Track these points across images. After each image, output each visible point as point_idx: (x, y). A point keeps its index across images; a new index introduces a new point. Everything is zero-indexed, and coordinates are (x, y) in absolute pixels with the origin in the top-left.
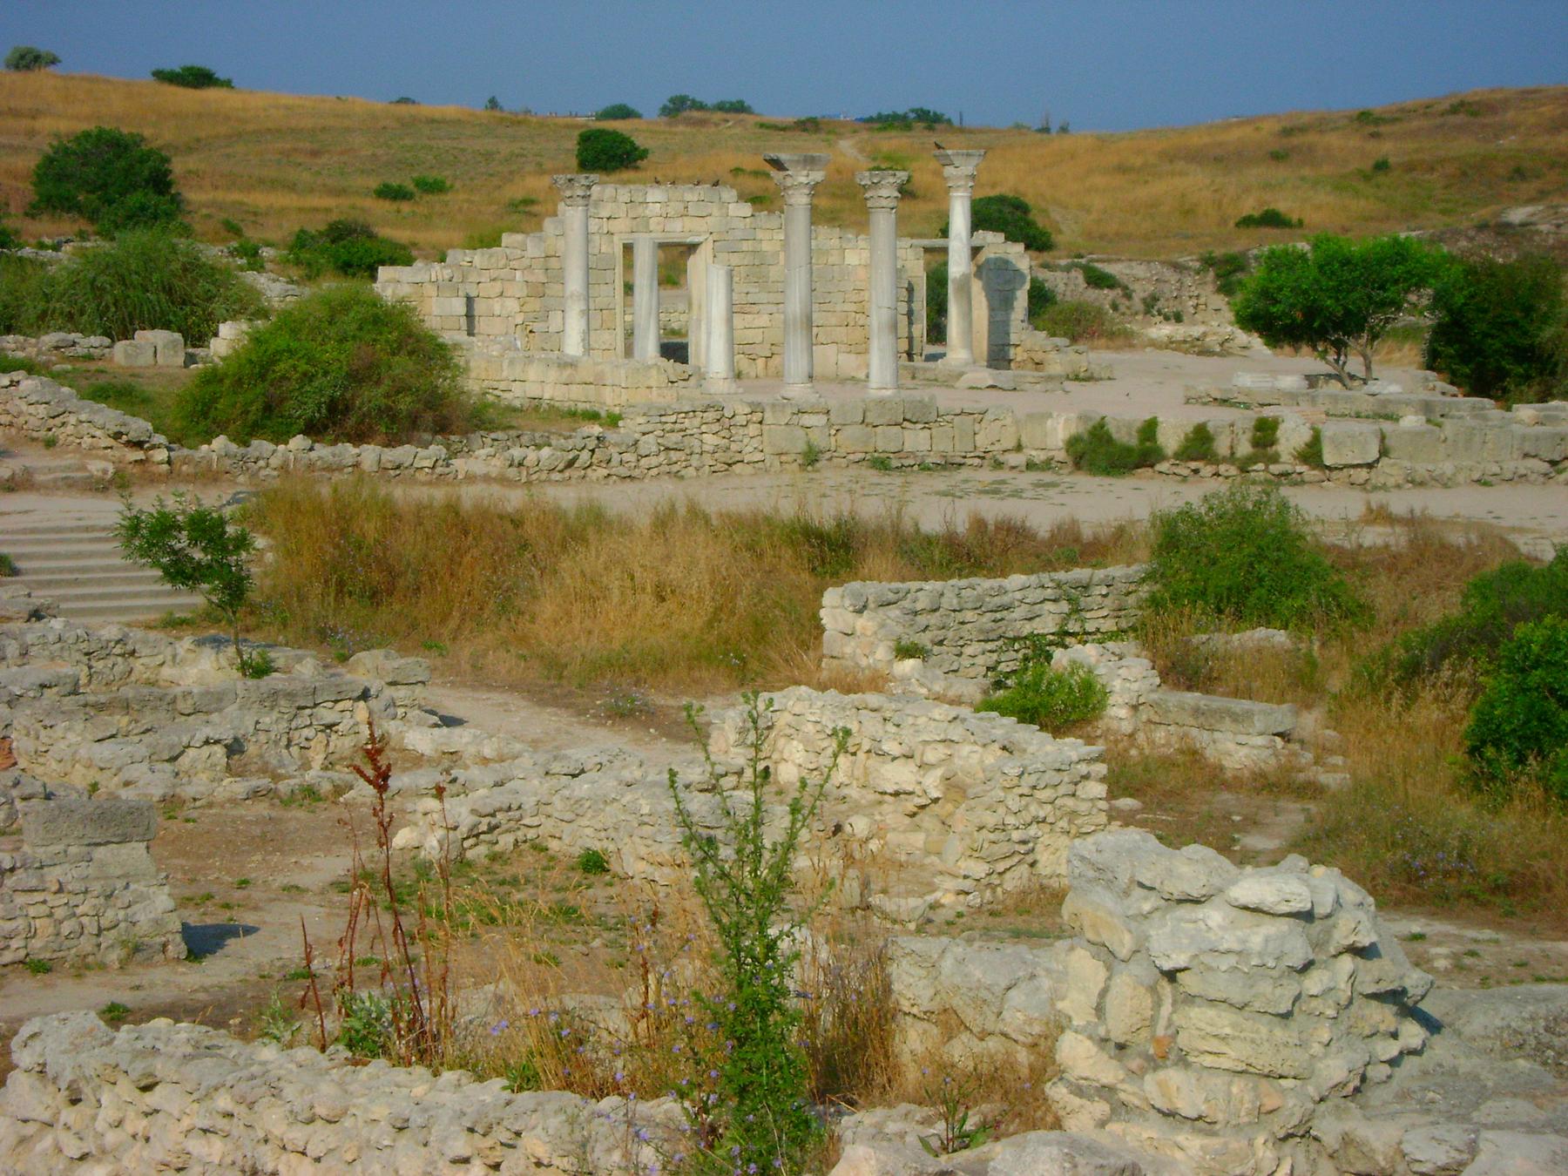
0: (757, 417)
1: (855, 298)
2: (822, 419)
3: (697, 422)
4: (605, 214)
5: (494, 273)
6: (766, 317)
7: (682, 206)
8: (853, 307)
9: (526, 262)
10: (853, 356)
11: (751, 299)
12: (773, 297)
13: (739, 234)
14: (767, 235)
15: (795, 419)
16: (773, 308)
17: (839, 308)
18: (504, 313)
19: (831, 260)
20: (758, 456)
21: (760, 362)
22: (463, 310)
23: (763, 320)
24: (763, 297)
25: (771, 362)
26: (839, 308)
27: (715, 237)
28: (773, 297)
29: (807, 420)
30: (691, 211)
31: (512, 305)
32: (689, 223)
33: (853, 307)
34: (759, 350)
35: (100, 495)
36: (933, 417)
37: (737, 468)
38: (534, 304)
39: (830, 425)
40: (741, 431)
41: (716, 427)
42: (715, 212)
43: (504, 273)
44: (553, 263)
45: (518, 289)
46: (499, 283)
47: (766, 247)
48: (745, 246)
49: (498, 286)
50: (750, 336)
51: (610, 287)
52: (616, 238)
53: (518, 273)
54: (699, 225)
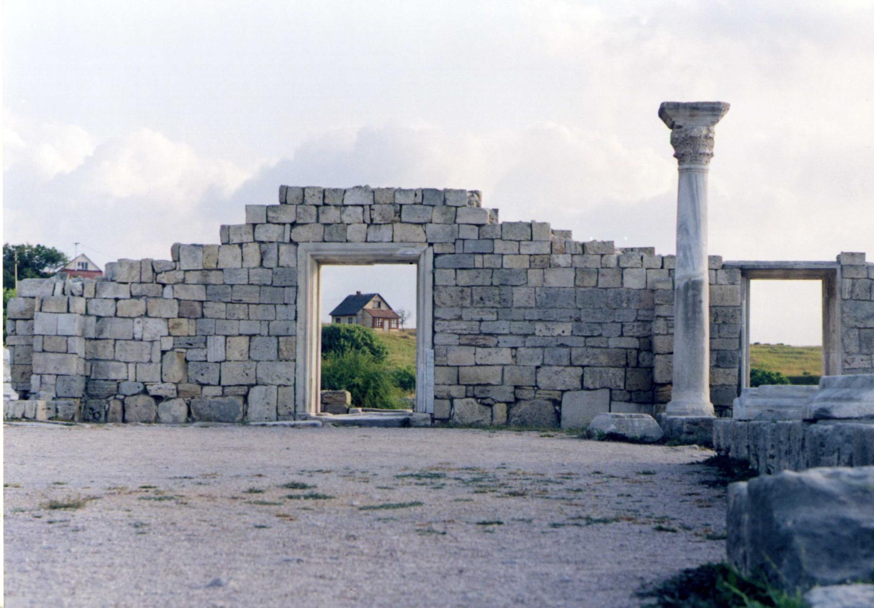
1: (638, 331)
4: (291, 219)
5: (137, 289)
8: (634, 343)
9: (180, 276)
11: (485, 328)
12: (516, 327)
13: (470, 247)
17: (613, 343)
18: (147, 336)
21: (500, 410)
24: (503, 326)
25: (515, 411)
27: (437, 249)
28: (516, 327)
30: (404, 218)
38: (187, 327)
46: (142, 301)
47: (508, 262)
49: (140, 306)
51: (291, 309)
52: (301, 247)
53: (168, 291)
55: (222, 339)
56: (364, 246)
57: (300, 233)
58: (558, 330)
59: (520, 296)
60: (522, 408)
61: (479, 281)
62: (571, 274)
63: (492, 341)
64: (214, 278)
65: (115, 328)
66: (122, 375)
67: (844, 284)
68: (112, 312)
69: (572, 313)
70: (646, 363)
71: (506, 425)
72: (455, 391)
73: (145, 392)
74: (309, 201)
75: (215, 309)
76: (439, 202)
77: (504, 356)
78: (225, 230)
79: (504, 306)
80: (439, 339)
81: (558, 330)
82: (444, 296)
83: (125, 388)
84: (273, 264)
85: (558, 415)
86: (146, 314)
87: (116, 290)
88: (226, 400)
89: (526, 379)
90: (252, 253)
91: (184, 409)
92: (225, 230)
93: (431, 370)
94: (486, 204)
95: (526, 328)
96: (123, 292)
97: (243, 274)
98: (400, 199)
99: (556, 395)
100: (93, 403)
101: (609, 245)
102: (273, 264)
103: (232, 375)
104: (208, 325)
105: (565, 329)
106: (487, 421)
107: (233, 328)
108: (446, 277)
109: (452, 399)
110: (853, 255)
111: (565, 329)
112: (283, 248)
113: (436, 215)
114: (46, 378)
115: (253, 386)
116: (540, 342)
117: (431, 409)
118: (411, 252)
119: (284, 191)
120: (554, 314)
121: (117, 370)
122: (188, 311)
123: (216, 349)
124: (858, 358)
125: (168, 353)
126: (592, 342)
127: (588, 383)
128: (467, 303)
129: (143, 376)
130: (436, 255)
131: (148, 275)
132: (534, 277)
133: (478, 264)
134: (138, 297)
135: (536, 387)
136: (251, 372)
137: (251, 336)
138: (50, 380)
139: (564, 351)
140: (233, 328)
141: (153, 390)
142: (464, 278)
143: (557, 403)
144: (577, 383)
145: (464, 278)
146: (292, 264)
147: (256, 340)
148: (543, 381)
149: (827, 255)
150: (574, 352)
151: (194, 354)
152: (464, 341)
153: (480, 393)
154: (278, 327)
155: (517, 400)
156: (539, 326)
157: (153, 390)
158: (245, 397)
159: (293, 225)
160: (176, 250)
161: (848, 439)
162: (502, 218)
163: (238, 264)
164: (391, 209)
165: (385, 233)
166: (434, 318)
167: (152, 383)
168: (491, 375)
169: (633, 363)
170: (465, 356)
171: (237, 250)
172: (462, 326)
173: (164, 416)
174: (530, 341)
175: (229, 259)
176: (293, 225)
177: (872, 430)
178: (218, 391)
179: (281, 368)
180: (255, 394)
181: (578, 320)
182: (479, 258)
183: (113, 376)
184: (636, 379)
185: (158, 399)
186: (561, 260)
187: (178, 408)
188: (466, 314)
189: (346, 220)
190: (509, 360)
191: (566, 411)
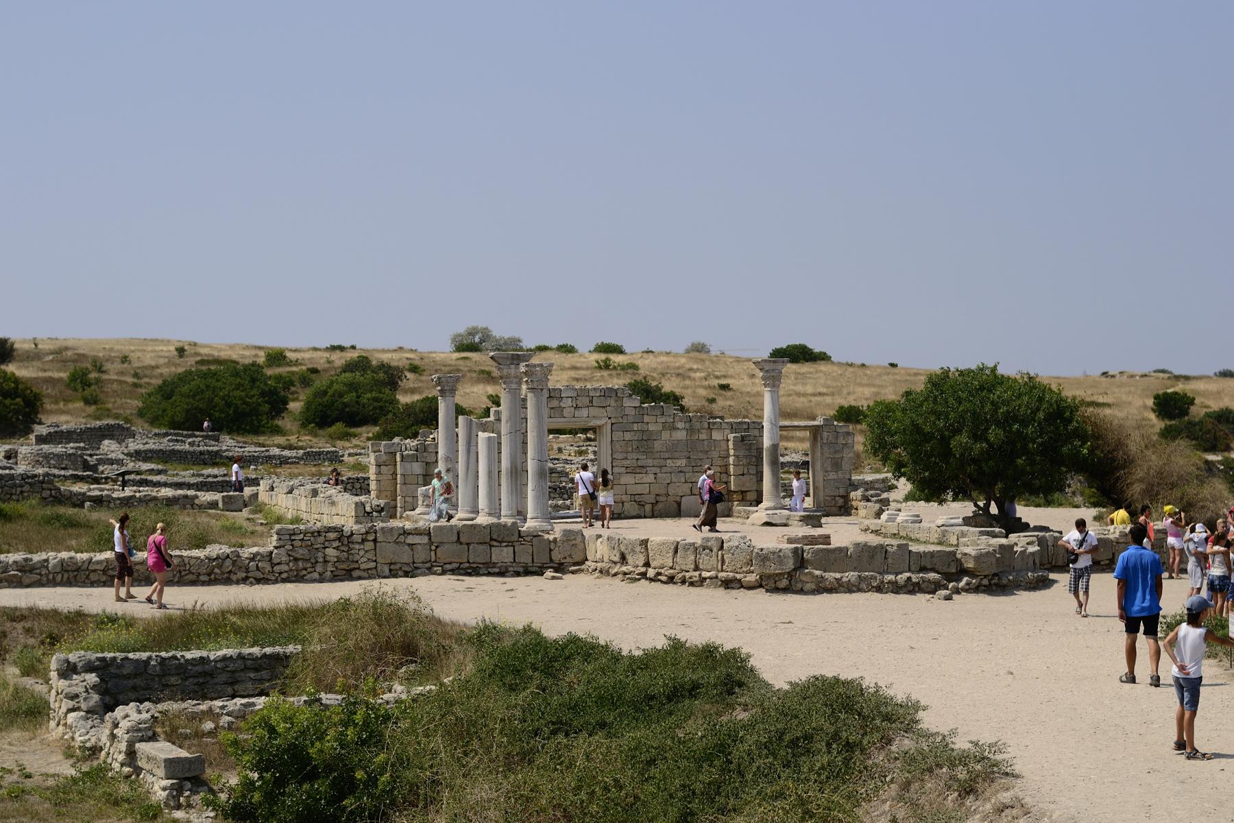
0: (371, 537)
1: (719, 462)
2: (425, 540)
3: (321, 539)
6: (652, 476)
7: (587, 400)
8: (719, 469)
11: (639, 463)
12: (656, 462)
13: (631, 419)
15: (402, 539)
16: (658, 470)
19: (703, 436)
20: (372, 565)
21: (648, 507)
24: (650, 462)
28: (656, 462)
29: (410, 540)
32: (593, 411)
36: (515, 537)
37: (355, 574)
39: (431, 543)
40: (357, 546)
41: (336, 544)
42: (613, 403)
47: (651, 427)
48: (635, 427)
50: (639, 489)
58: (679, 463)
59: (657, 445)
60: (660, 506)
62: (684, 433)
71: (653, 516)
72: (624, 498)
80: (616, 470)
81: (679, 463)
82: (617, 446)
89: (663, 491)
95: (662, 462)
99: (678, 499)
105: (682, 462)
108: (618, 435)
111: (682, 462)
113: (612, 402)
118: (599, 423)
120: (677, 455)
126: (696, 469)
132: (665, 435)
142: (628, 436)
143: (679, 504)
145: (628, 436)
148: (671, 491)
165: (584, 412)
168: (644, 489)
174: (664, 470)
186: (680, 425)
188: (630, 456)
189: (563, 405)
191: (683, 507)
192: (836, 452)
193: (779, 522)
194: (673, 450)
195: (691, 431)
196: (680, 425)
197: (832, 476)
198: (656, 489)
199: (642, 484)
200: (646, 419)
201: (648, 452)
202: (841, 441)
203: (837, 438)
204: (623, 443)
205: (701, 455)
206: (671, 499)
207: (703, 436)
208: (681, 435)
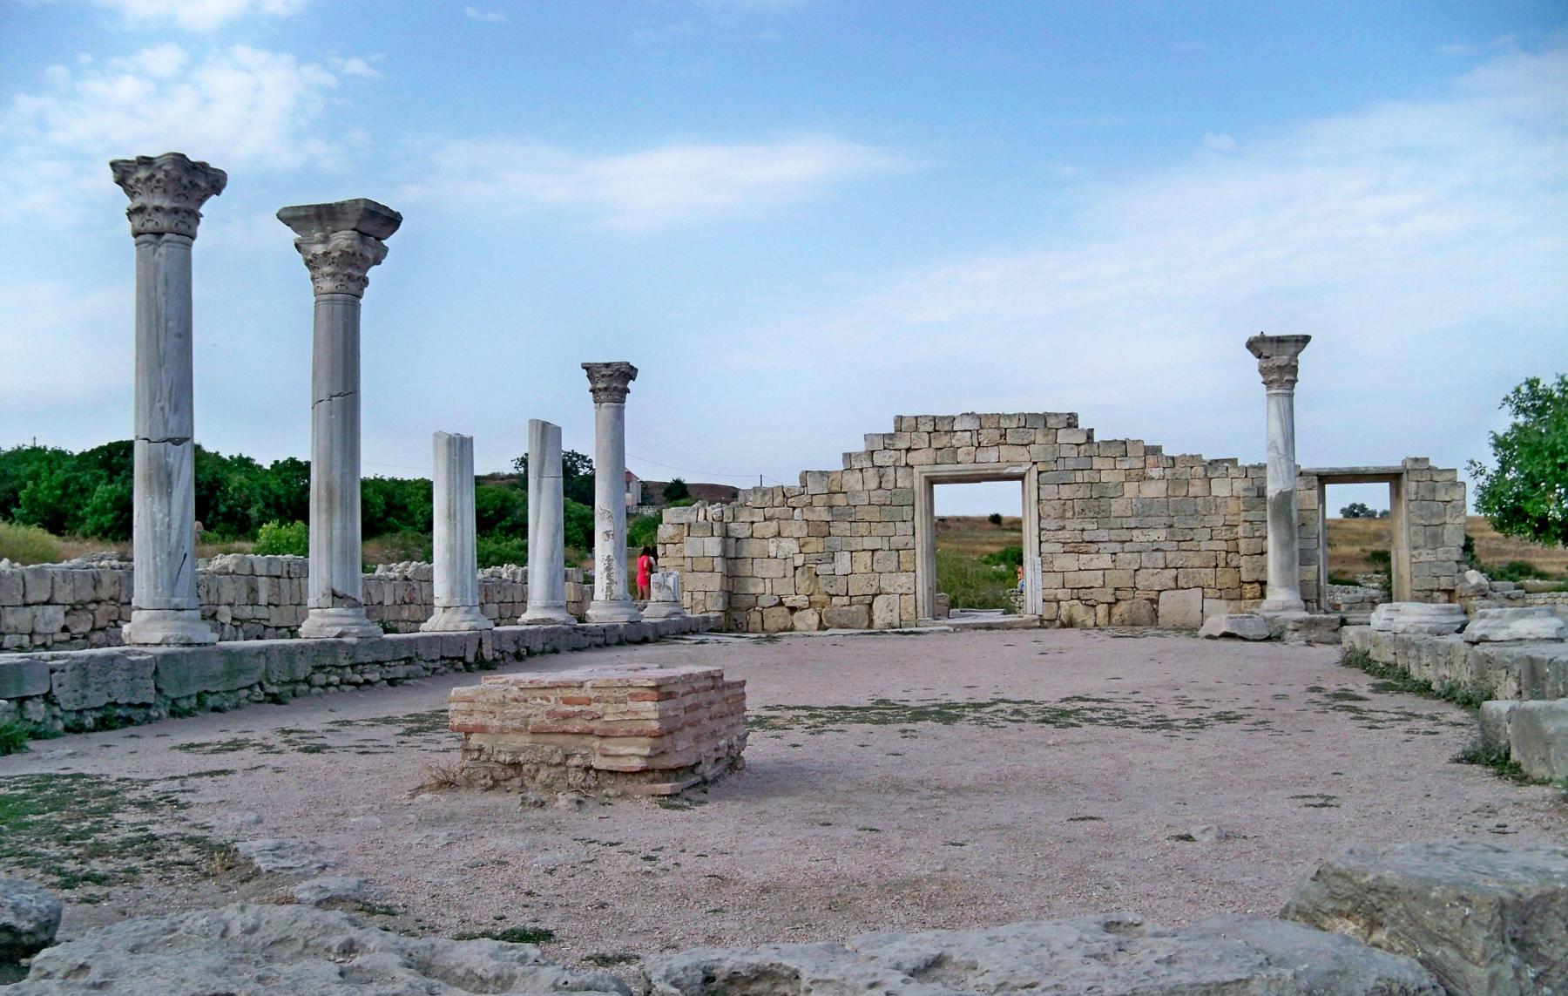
4: (903, 445)
5: (769, 512)
6: (1108, 558)
8: (1224, 546)
9: (806, 499)
10: (1223, 602)
12: (1114, 535)
13: (1071, 464)
14: (1109, 463)
16: (1118, 547)
17: (1203, 546)
18: (781, 555)
19: (1197, 488)
21: (1102, 610)
22: (717, 551)
23: (1105, 561)
24: (1103, 534)
25: (1116, 610)
26: (1203, 546)
27: (1041, 467)
28: (1114, 535)
30: (1009, 440)
31: (790, 546)
33: (1224, 546)
34: (1097, 595)
35: (77, 737)
38: (815, 545)
42: (1040, 438)
43: (777, 512)
44: (839, 500)
45: (795, 528)
47: (1105, 477)
49: (772, 527)
50: (1086, 578)
54: (1020, 454)
55: (847, 555)
56: (973, 466)
57: (913, 458)
58: (1153, 535)
59: (1117, 506)
60: (1122, 608)
61: (1080, 495)
62: (1162, 485)
63: (1094, 547)
64: (839, 500)
65: (751, 548)
66: (760, 589)
67: (1410, 486)
68: (748, 534)
69: (1166, 520)
70: (1234, 564)
72: (1061, 594)
73: (781, 604)
74: (922, 428)
75: (841, 528)
76: (1041, 424)
77: (1105, 561)
78: (848, 457)
79: (1102, 516)
81: (1153, 535)
82: (1047, 509)
83: (763, 601)
84: (891, 486)
85: (1156, 611)
86: (779, 535)
87: (752, 514)
88: (853, 608)
90: (871, 474)
91: (816, 618)
92: (848, 457)
93: (1039, 576)
94: (1083, 424)
95: (1125, 535)
96: (758, 516)
97: (865, 496)
98: (1004, 424)
99: (1153, 595)
100: (735, 615)
101: (1195, 459)
102: (891, 486)
103: (858, 586)
104: (835, 542)
105: (1162, 534)
106: (1090, 622)
107: (857, 543)
108: (1049, 491)
109: (1058, 602)
110: (1416, 460)
112: (900, 471)
114: (696, 595)
115: (874, 596)
116: (1137, 547)
117: (1040, 612)
118: (1016, 470)
119: (899, 419)
121: (755, 585)
122: (821, 531)
123: (843, 563)
124: (1424, 552)
125: (799, 572)
126: (1184, 546)
127: (1181, 583)
128: (1069, 514)
129: (778, 590)
130: (1039, 473)
131: (779, 499)
132: (1130, 489)
133: (1079, 480)
134: (770, 519)
135: (1135, 588)
136: (875, 583)
137: (873, 551)
138: (699, 596)
139: (1160, 554)
140: (857, 543)
141: (788, 601)
142: (1066, 492)
143: (1154, 601)
144: (1172, 585)
146: (907, 484)
147: (878, 554)
148: (1142, 580)
149: (1393, 462)
150: (1170, 556)
151: (823, 569)
152: (1067, 548)
153: (1081, 594)
154: (897, 541)
155: (1118, 600)
156: (1135, 532)
157: (788, 601)
158: (870, 605)
159: (908, 450)
160: (804, 476)
161: (1518, 661)
162: (1096, 439)
163: (859, 487)
164: (997, 433)
166: (1041, 530)
167: (787, 596)
169: (1222, 564)
170: (1069, 562)
171: (859, 475)
172: (1064, 535)
173: (798, 625)
175: (853, 482)
176: (908, 450)
177: (1564, 658)
178: (846, 600)
179: (903, 579)
180: (879, 603)
181: (1171, 526)
182: (1079, 474)
183: (752, 590)
184: (1227, 578)
185: (793, 610)
186: (1155, 473)
187: (811, 618)
188: (1067, 523)
190: (1111, 565)
191: (1162, 610)
192: (1432, 515)
193: (1250, 635)
194: (1144, 510)
195: (1174, 482)
196: (1155, 473)
197: (1426, 556)
198: (1115, 579)
199: (1095, 568)
200: (1097, 463)
201: (1102, 516)
202: (1442, 495)
203: (1433, 490)
204: (1057, 504)
205: (1192, 523)
206: (1141, 595)
207: (1197, 488)
208: (1154, 490)
